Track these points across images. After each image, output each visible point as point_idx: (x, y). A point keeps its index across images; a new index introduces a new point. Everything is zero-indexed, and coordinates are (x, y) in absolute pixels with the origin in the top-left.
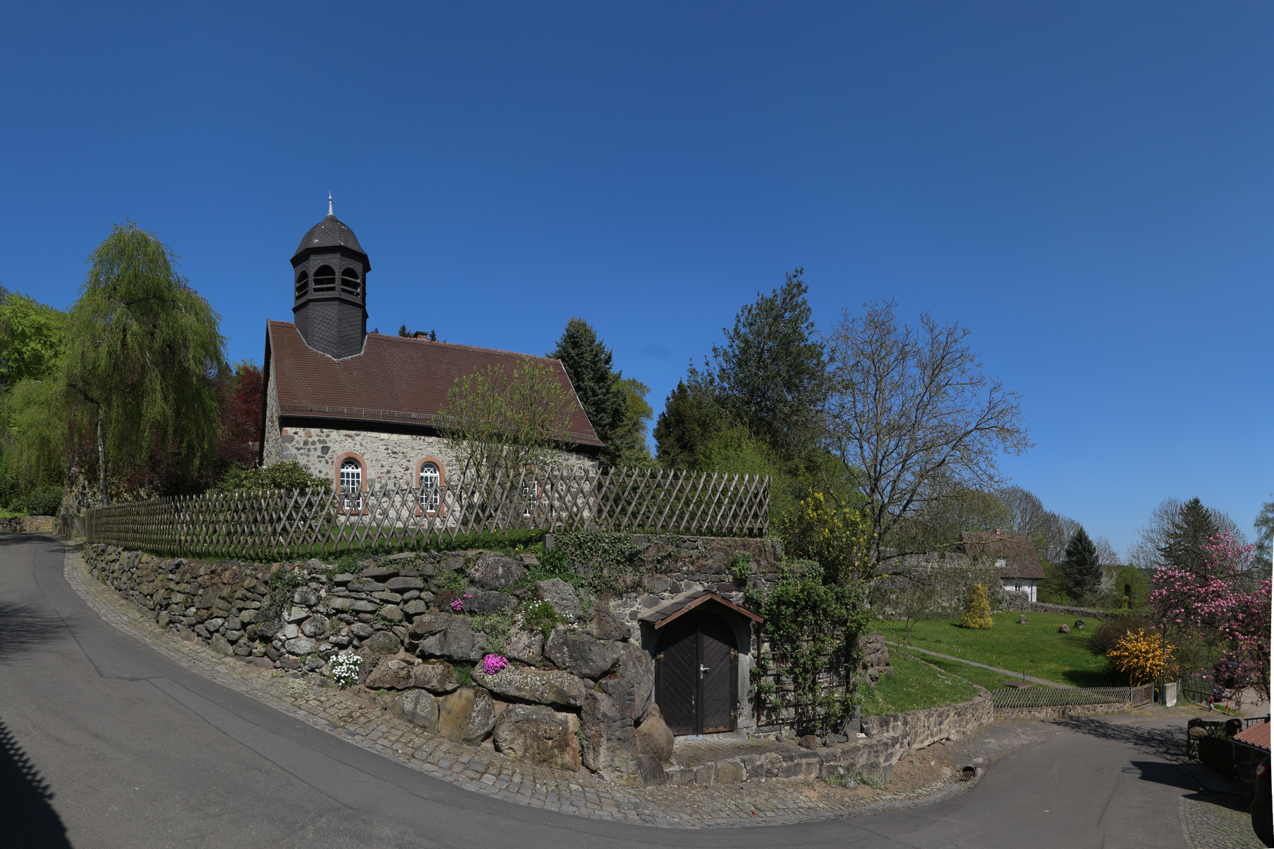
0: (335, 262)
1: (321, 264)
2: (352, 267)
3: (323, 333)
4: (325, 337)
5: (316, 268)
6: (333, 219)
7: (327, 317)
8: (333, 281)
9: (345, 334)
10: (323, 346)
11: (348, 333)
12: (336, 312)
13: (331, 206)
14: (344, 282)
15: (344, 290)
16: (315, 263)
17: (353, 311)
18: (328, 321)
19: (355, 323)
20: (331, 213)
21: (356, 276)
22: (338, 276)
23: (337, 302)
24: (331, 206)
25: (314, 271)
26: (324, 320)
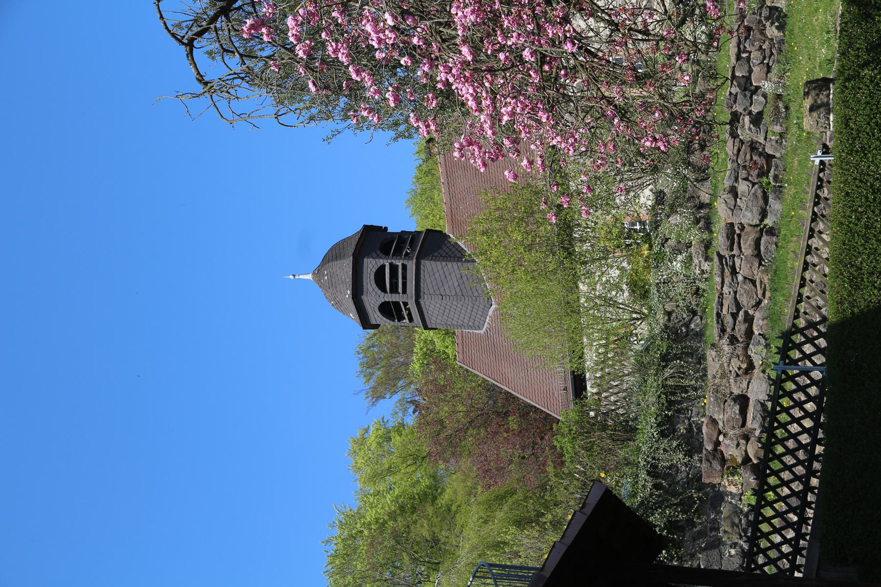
0: (373, 298)
1: (379, 314)
2: (373, 277)
3: (462, 315)
4: (468, 314)
5: (385, 319)
6: (318, 273)
7: (441, 311)
8: (396, 304)
9: (458, 289)
10: (479, 316)
11: (456, 284)
12: (433, 302)
13: (301, 277)
14: (394, 289)
15: (404, 292)
16: (376, 317)
17: (427, 276)
18: (447, 311)
19: (441, 272)
20: (309, 277)
21: (383, 267)
22: (389, 298)
23: (422, 301)
24: (301, 277)
25: (388, 321)
26: (445, 314)
